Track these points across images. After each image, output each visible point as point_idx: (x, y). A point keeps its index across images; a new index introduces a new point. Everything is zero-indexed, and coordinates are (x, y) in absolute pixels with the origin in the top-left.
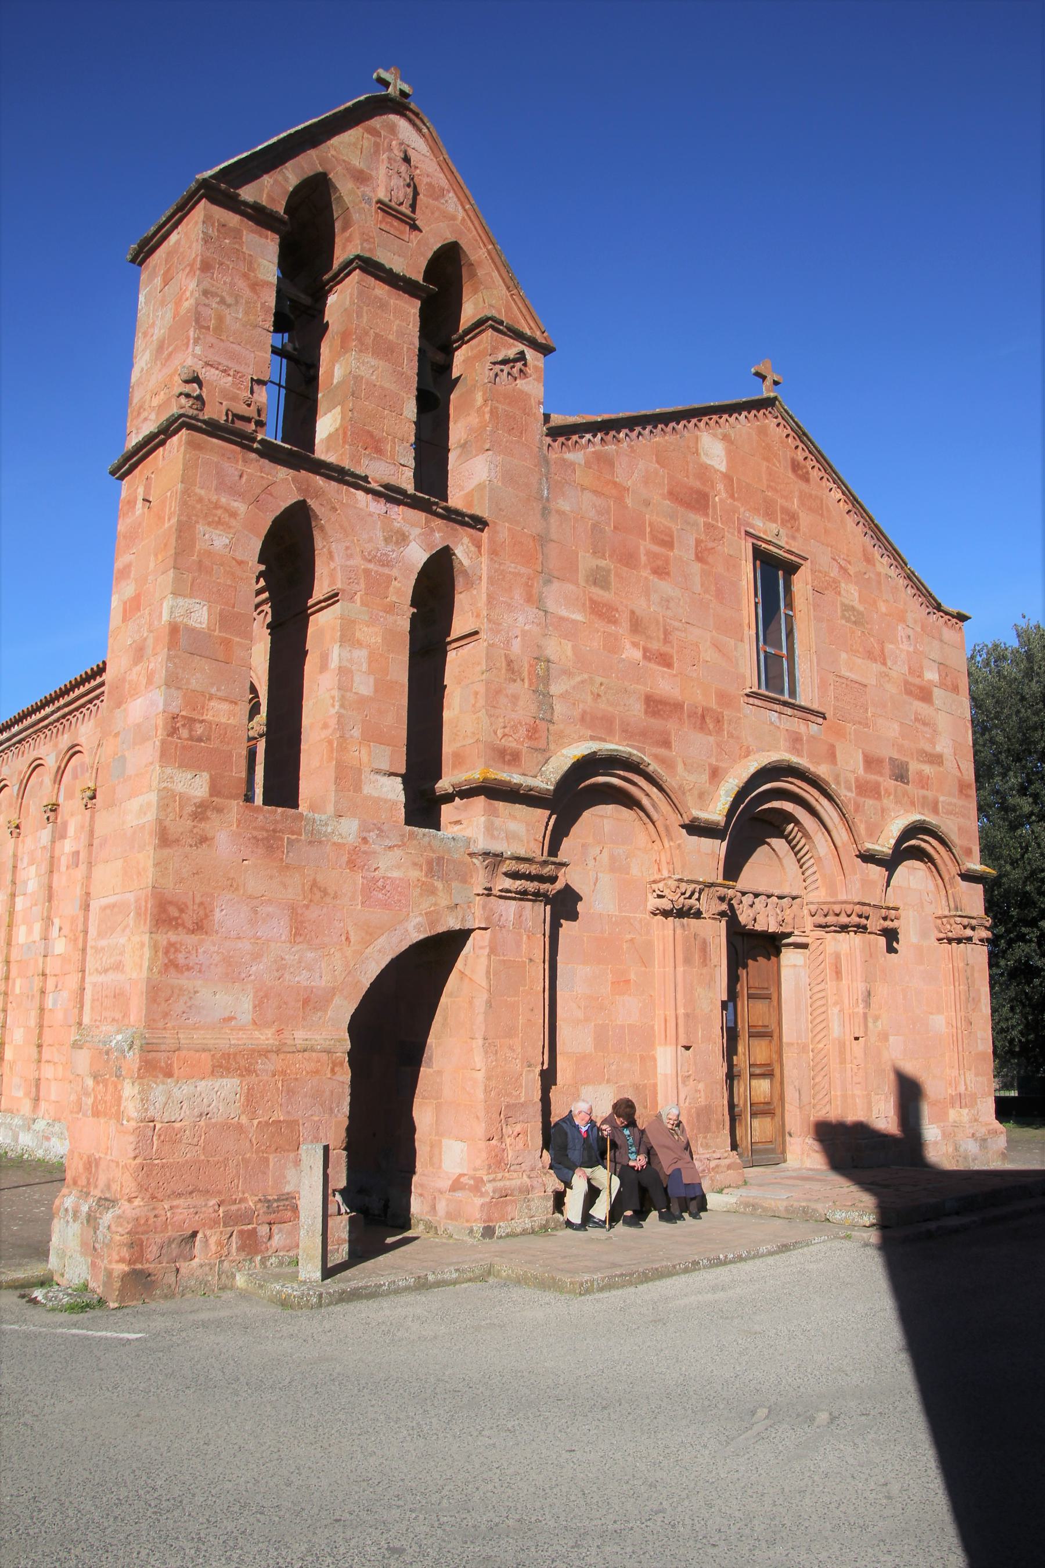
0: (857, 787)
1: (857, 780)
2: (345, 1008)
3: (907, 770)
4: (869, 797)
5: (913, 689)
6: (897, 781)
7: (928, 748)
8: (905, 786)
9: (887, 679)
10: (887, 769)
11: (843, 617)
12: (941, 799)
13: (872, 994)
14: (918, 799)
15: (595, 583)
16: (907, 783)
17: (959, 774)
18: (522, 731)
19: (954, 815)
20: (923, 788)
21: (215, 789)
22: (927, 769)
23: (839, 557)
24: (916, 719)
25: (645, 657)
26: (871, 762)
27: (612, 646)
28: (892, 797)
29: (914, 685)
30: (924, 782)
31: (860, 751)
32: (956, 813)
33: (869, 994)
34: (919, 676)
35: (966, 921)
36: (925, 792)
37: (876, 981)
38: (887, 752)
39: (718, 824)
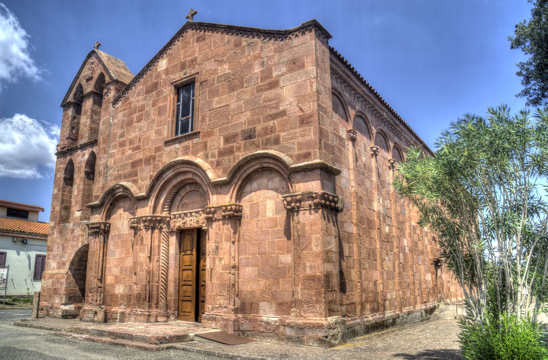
0: (218, 154)
1: (219, 151)
2: (68, 265)
3: (255, 131)
4: (226, 155)
5: (263, 87)
6: (246, 140)
7: (273, 111)
8: (252, 140)
9: (244, 93)
10: (240, 138)
11: (218, 82)
12: (282, 134)
13: (219, 248)
14: (262, 142)
15: (121, 138)
16: (255, 137)
17: (301, 114)
18: (100, 189)
19: (294, 139)
20: (267, 134)
21: (55, 224)
22: (271, 123)
23: (219, 58)
24: (264, 102)
25: (133, 151)
26: (227, 140)
27: (123, 153)
28: (242, 149)
29: (264, 85)
30: (266, 131)
31: (222, 137)
32: (296, 137)
33: (217, 248)
34: (270, 78)
35: (289, 199)
36: (268, 136)
37: (222, 242)
38: (239, 130)
39: (143, 196)
